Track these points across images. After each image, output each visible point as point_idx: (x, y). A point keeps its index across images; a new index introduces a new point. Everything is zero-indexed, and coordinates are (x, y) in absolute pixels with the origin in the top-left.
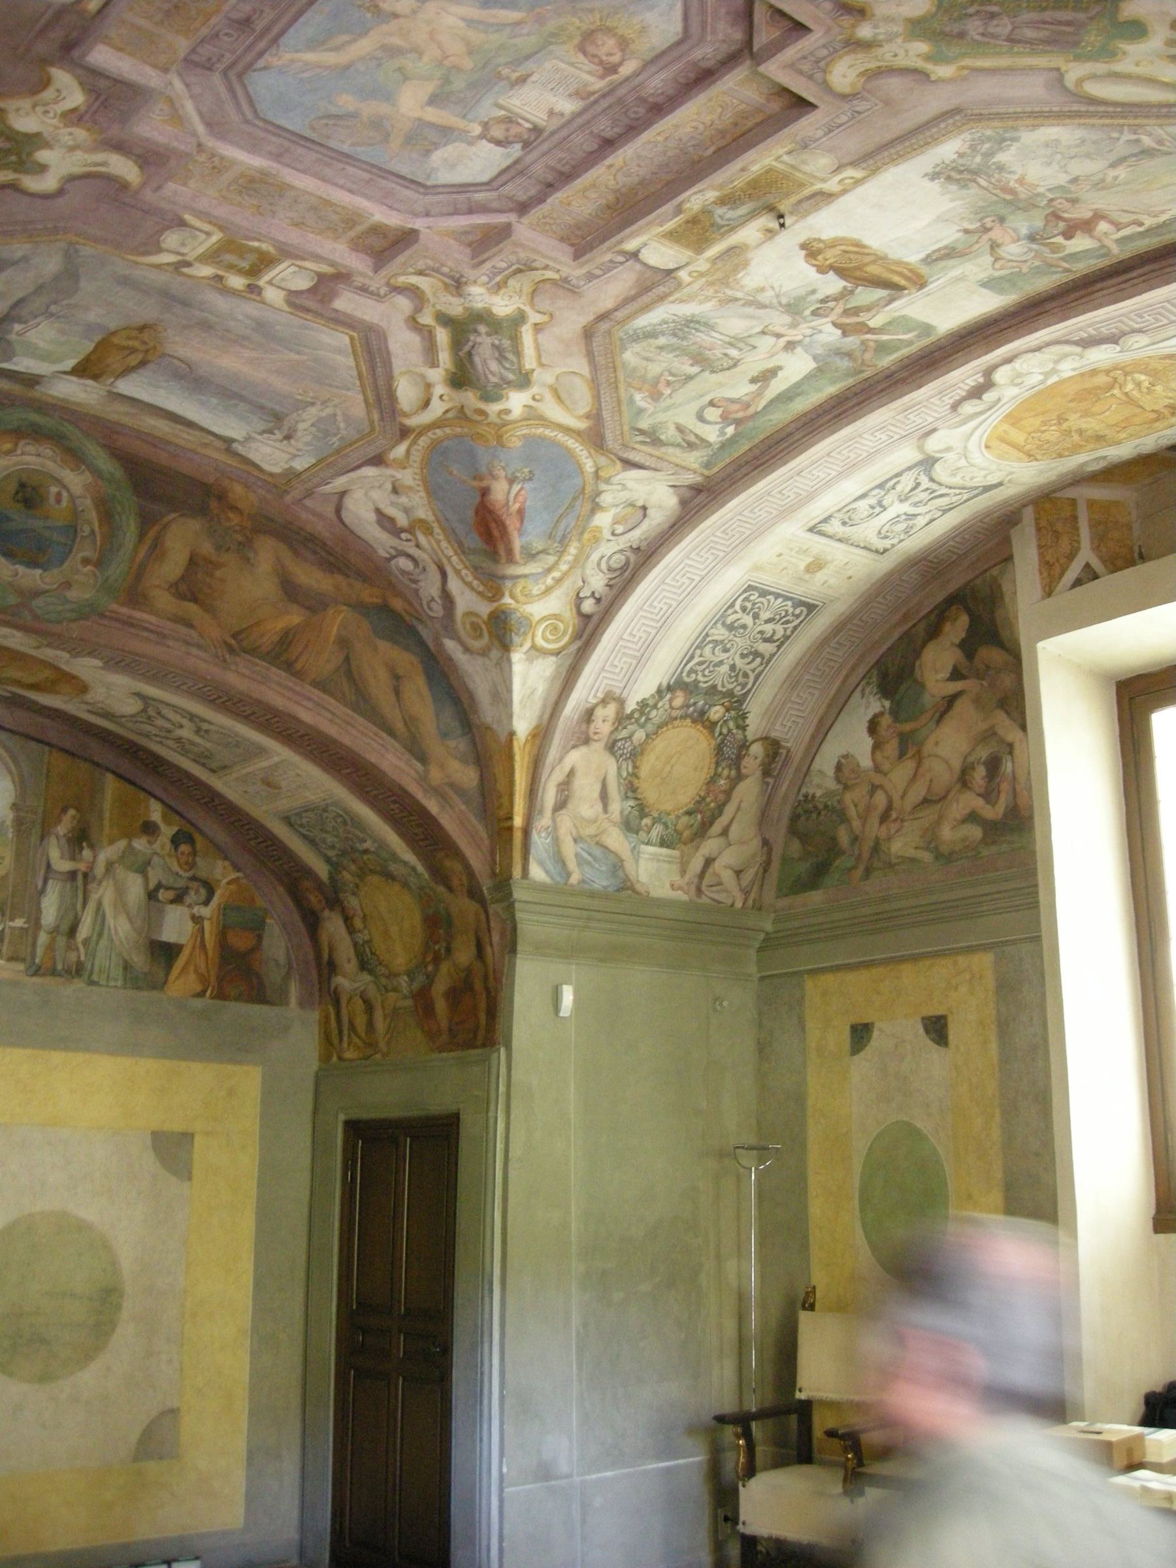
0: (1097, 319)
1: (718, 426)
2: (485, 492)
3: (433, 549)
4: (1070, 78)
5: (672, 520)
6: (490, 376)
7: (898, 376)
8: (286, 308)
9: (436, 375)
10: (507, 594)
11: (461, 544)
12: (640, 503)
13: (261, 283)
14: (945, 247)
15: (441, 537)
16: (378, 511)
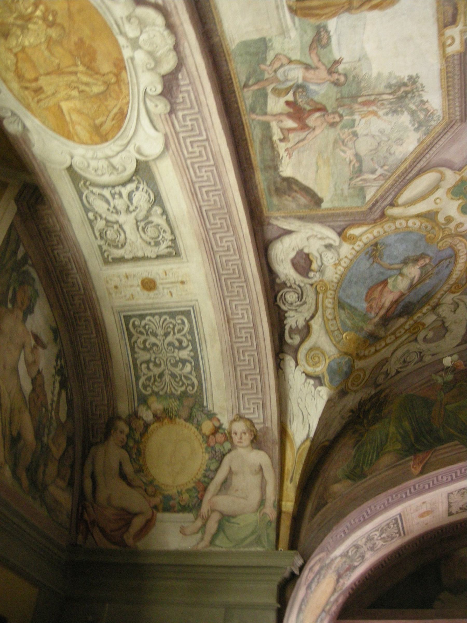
0: (202, 98)
4: (449, 173)
14: (329, 43)
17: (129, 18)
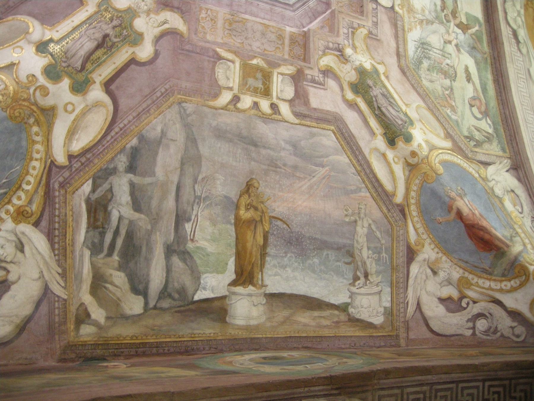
1: (484, 120)
2: (459, 214)
3: (482, 293)
5: (526, 193)
6: (397, 120)
7: (496, 56)
8: (297, 121)
9: (380, 143)
10: (527, 265)
11: (485, 271)
12: (510, 190)
13: (275, 100)
15: (476, 280)
16: (442, 300)
17: (519, 27)
